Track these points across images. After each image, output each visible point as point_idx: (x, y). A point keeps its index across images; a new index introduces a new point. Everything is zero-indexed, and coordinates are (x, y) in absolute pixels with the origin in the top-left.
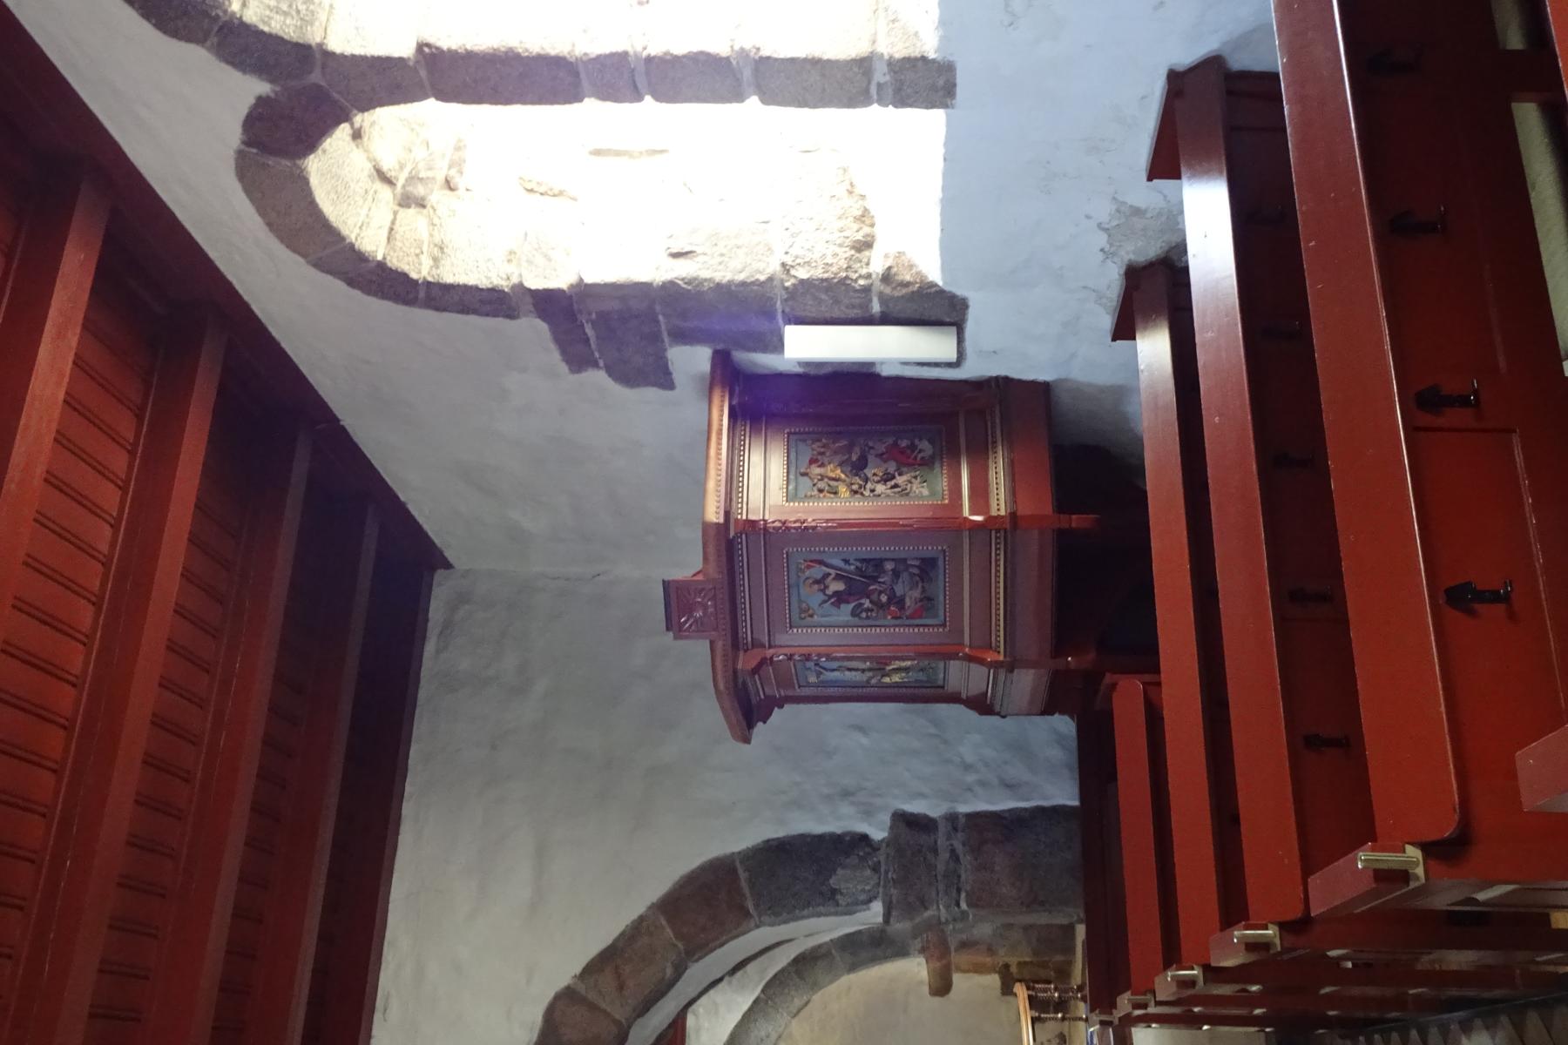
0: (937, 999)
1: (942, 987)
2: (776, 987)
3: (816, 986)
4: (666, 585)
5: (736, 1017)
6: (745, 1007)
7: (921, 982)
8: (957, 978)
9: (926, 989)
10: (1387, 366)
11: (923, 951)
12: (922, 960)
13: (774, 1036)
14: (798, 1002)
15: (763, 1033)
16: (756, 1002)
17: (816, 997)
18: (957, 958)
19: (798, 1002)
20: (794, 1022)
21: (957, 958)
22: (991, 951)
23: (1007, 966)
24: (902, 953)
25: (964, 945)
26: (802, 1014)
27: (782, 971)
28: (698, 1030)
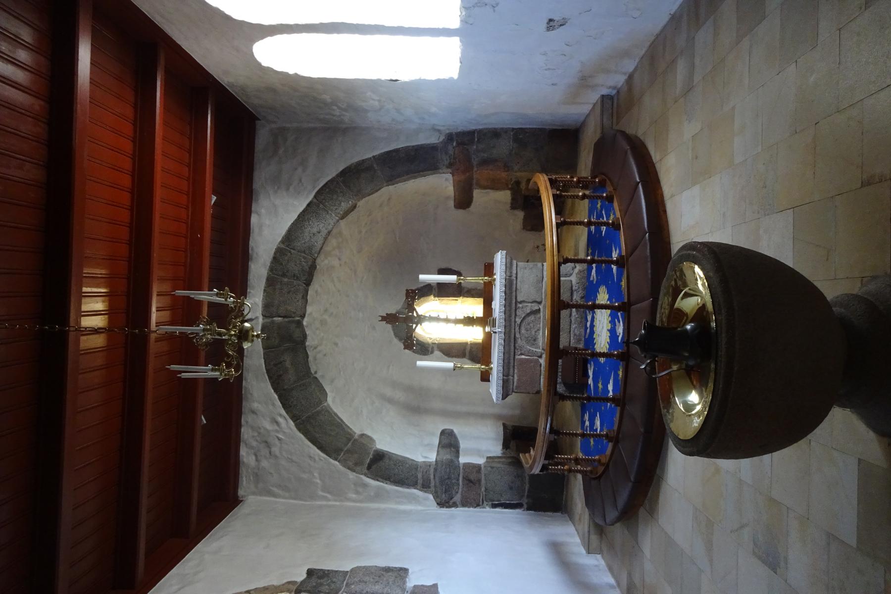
0: (461, 211)
1: (464, 201)
2: (325, 196)
3: (361, 194)
4: (406, 571)
5: (294, 216)
6: (301, 209)
7: (448, 198)
8: (477, 193)
9: (451, 203)
10: (643, 218)
11: (450, 165)
12: (450, 176)
13: (324, 232)
14: (345, 206)
15: (315, 230)
16: (309, 205)
17: (361, 203)
18: (478, 174)
19: (345, 206)
20: (343, 223)
21: (478, 174)
22: (507, 167)
23: (518, 183)
24: (433, 168)
25: (485, 162)
26: (350, 217)
27: (331, 181)
28: (261, 227)
